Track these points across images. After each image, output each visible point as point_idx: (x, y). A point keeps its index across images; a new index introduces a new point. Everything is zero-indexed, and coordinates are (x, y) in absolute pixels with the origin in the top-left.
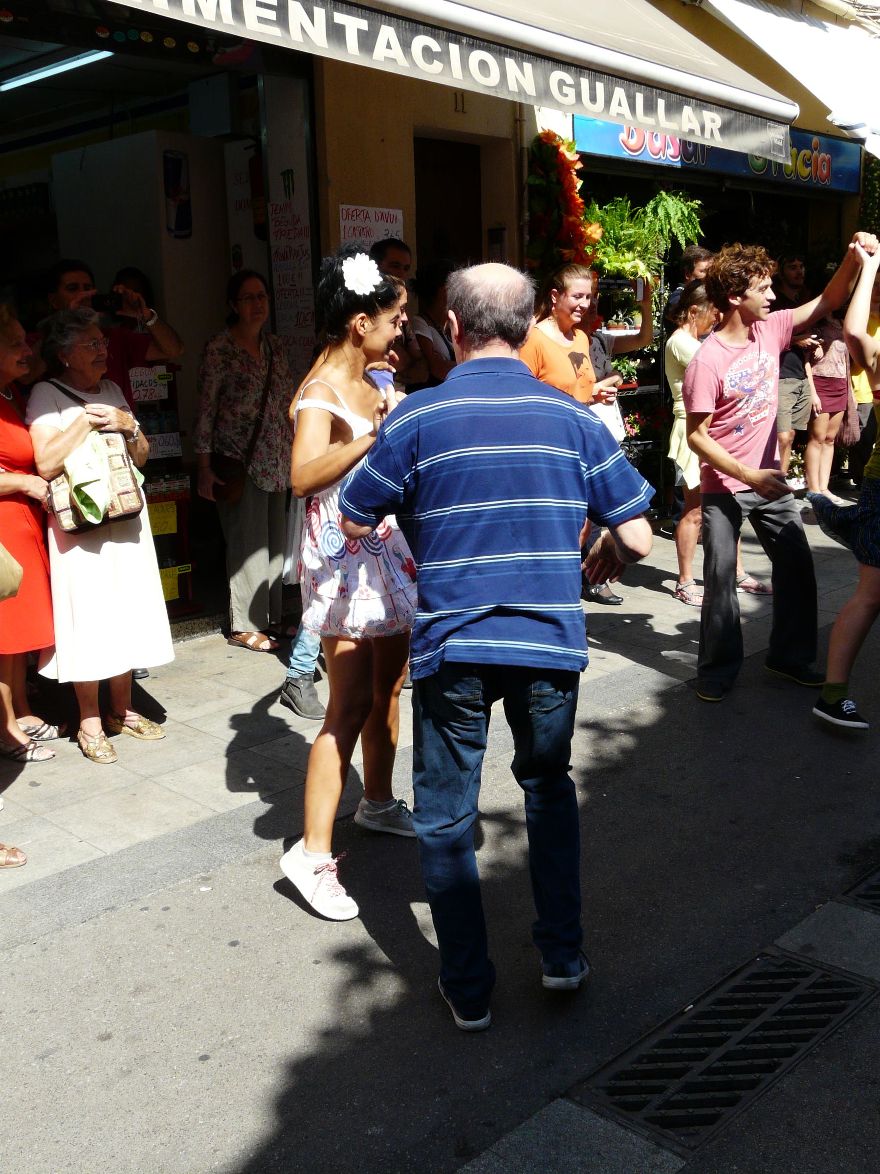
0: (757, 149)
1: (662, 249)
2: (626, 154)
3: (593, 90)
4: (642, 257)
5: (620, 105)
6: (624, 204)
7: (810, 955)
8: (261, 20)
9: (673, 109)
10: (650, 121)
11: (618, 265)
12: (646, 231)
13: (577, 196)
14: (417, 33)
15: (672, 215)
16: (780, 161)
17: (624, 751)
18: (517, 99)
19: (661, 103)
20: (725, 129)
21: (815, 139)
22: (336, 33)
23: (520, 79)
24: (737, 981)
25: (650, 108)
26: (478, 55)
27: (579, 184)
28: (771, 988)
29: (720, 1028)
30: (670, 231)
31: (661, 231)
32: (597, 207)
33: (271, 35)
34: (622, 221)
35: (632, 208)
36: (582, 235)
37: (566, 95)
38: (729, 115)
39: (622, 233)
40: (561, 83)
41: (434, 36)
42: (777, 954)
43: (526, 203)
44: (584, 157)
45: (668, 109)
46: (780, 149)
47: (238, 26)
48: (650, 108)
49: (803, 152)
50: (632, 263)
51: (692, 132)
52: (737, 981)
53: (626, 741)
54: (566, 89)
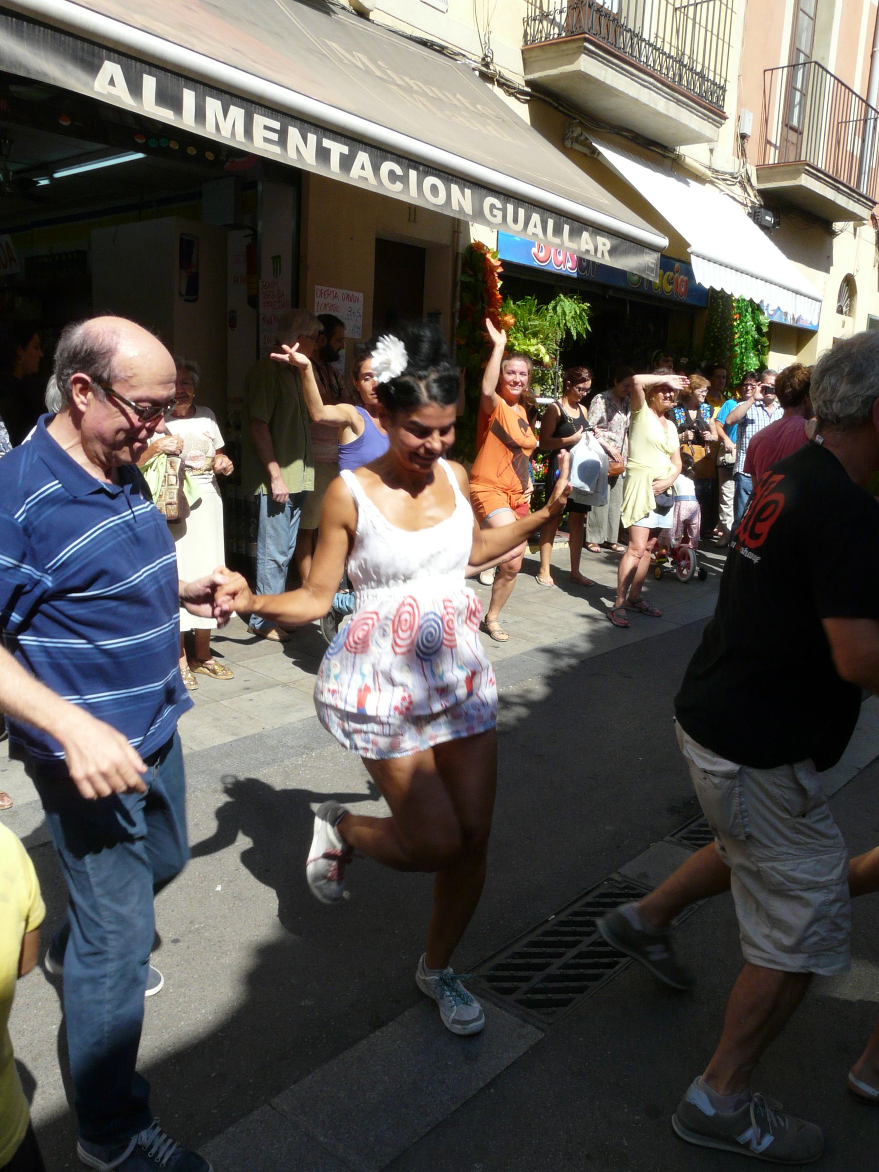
0: (636, 268)
1: (559, 337)
2: (536, 264)
3: (516, 214)
4: (543, 343)
5: (535, 226)
6: (532, 302)
8: (266, 140)
9: (575, 233)
10: (557, 240)
11: (525, 347)
13: (498, 293)
14: (386, 159)
15: (567, 312)
16: (651, 279)
18: (457, 216)
19: (566, 228)
20: (613, 252)
21: (677, 265)
22: (323, 154)
23: (461, 200)
25: (558, 231)
26: (430, 180)
27: (500, 284)
29: (574, 934)
30: (565, 324)
31: (559, 324)
33: (273, 152)
34: (530, 314)
35: (538, 305)
37: (495, 216)
38: (617, 241)
40: (493, 207)
41: (398, 163)
42: (619, 879)
43: (458, 294)
44: (505, 264)
46: (652, 270)
47: (248, 143)
48: (558, 231)
49: (668, 273)
50: (536, 347)
51: (588, 251)
52: (589, 899)
54: (495, 212)
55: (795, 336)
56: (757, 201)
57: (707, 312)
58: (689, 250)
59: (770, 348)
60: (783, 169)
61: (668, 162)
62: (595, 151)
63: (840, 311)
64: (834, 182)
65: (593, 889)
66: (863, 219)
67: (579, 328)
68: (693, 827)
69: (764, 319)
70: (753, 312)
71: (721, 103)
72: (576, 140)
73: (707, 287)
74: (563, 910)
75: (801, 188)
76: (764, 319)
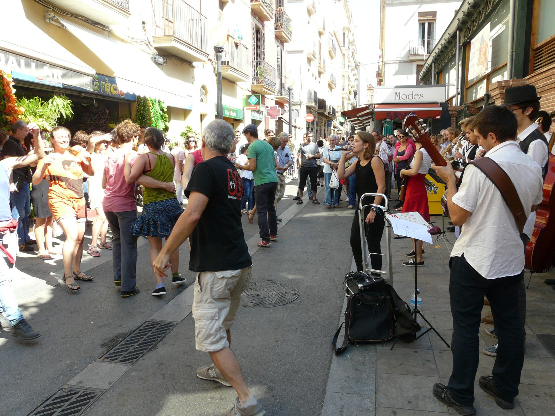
7: (80, 385)
12: (48, 111)
17: (32, 315)
20: (64, 76)
24: (48, 402)
25: (28, 65)
28: (62, 401)
30: (59, 111)
31: (55, 110)
32: (26, 100)
36: (16, 111)
38: (65, 71)
39: (37, 111)
44: (15, 80)
45: (37, 66)
46: (88, 85)
49: (113, 85)
51: (48, 76)
52: (48, 402)
53: (34, 310)
55: (185, 113)
56: (156, 52)
57: (136, 103)
58: (114, 75)
59: (170, 119)
60: (164, 38)
61: (106, 32)
62: (63, 26)
63: (202, 101)
64: (189, 45)
65: (51, 397)
66: (204, 61)
67: (68, 112)
68: (112, 351)
69: (165, 106)
70: (159, 102)
71: (127, 6)
72: (52, 19)
73: (125, 92)
74: (32, 412)
75: (173, 47)
76: (165, 106)
